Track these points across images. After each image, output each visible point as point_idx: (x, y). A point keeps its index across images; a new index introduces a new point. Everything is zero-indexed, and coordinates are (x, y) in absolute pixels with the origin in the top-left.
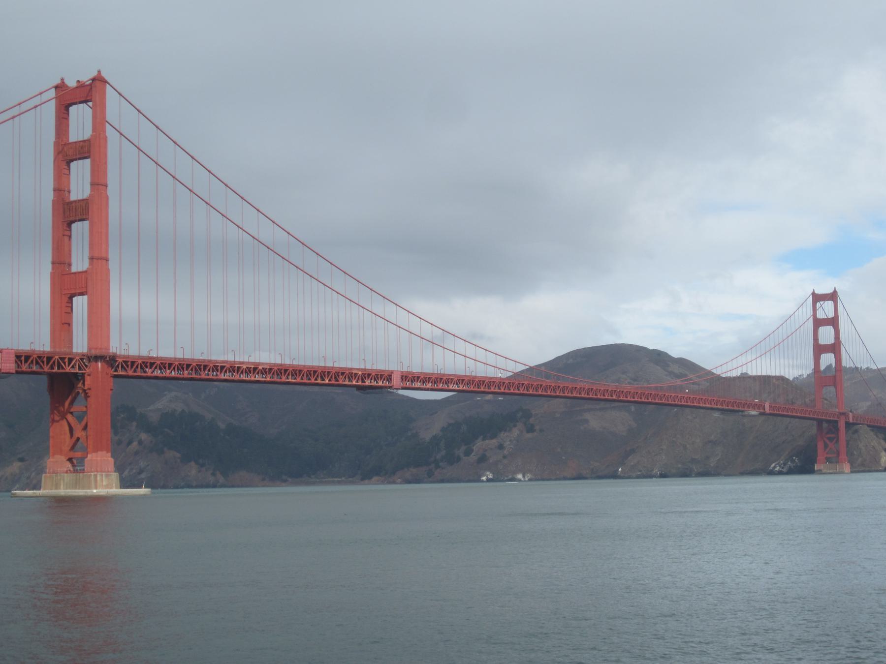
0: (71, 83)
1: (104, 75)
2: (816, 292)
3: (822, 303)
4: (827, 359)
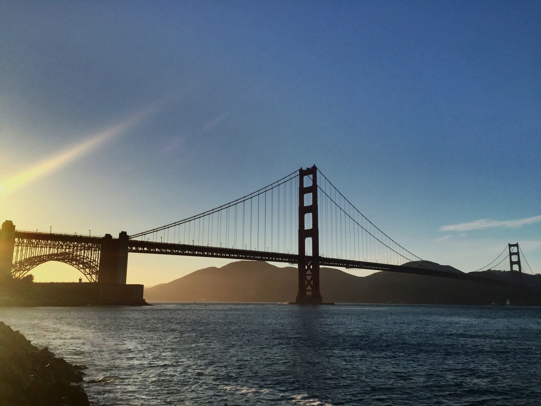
0: (304, 168)
1: (315, 166)
2: (510, 244)
3: (512, 248)
4: (516, 268)
